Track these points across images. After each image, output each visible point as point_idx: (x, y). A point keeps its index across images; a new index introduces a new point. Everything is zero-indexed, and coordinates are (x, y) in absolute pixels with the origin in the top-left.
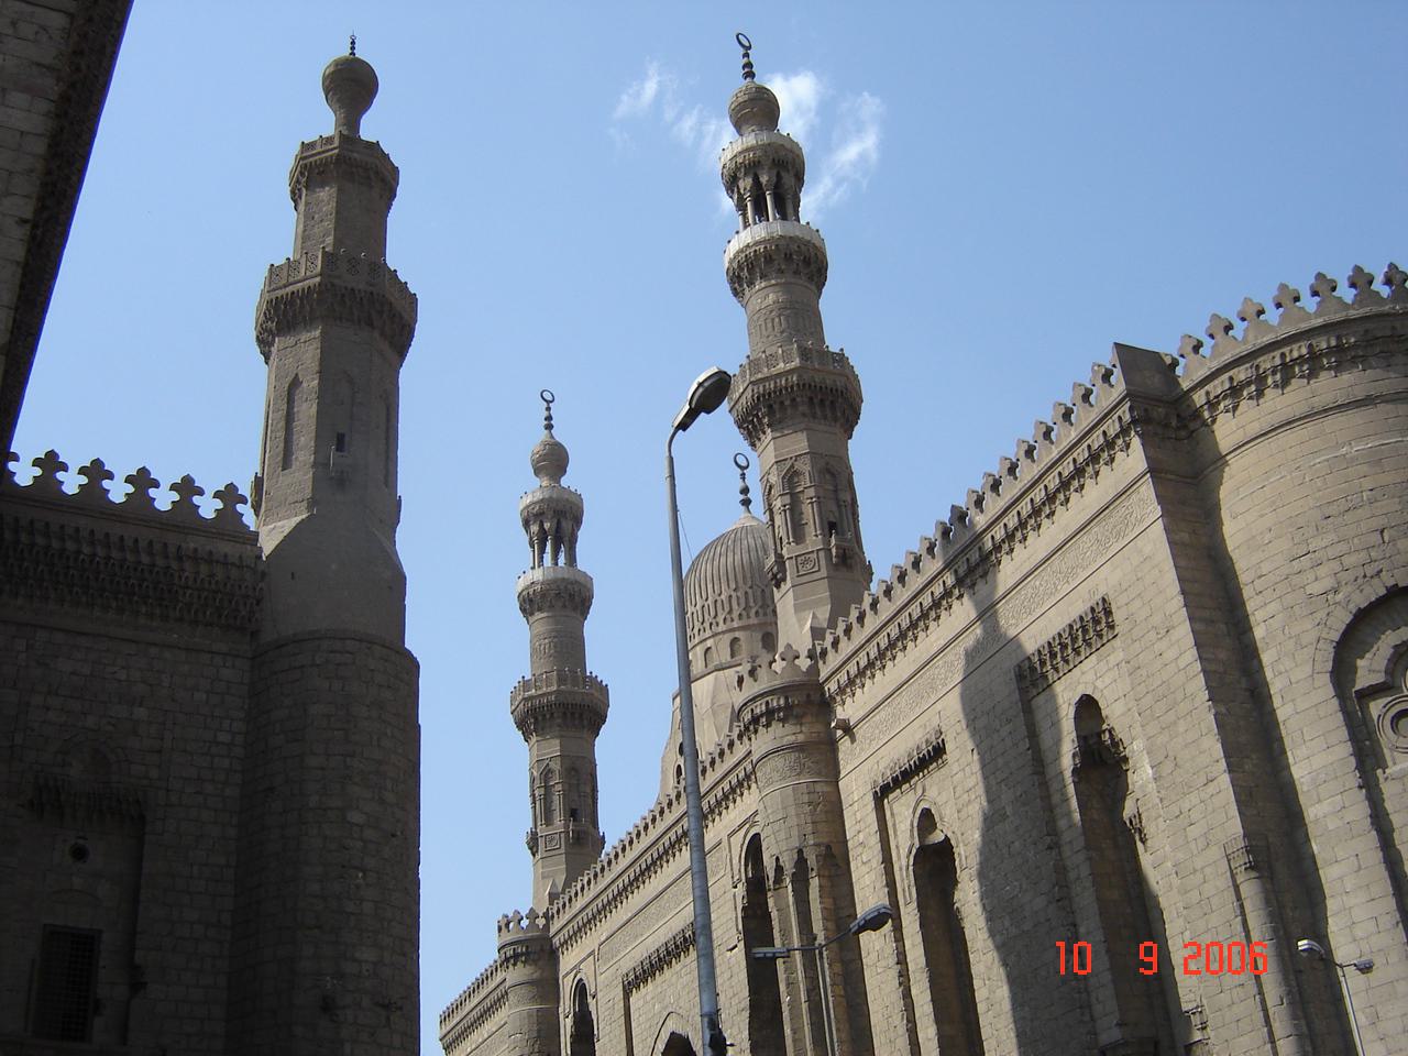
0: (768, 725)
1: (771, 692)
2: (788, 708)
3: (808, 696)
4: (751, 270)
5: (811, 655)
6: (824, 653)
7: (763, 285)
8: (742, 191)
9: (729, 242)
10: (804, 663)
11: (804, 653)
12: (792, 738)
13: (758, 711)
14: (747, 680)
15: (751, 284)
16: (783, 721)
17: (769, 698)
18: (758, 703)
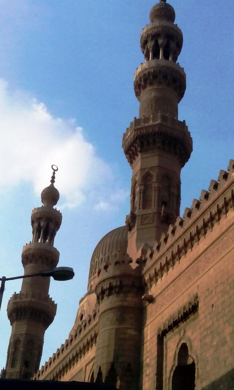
0: (109, 295)
1: (114, 277)
2: (121, 286)
3: (133, 282)
4: (145, 81)
5: (138, 262)
6: (145, 261)
7: (150, 88)
8: (149, 48)
9: (137, 69)
10: (134, 265)
11: (134, 260)
12: (120, 303)
13: (105, 288)
14: (103, 271)
15: (144, 87)
16: (118, 293)
17: (112, 281)
18: (105, 283)
